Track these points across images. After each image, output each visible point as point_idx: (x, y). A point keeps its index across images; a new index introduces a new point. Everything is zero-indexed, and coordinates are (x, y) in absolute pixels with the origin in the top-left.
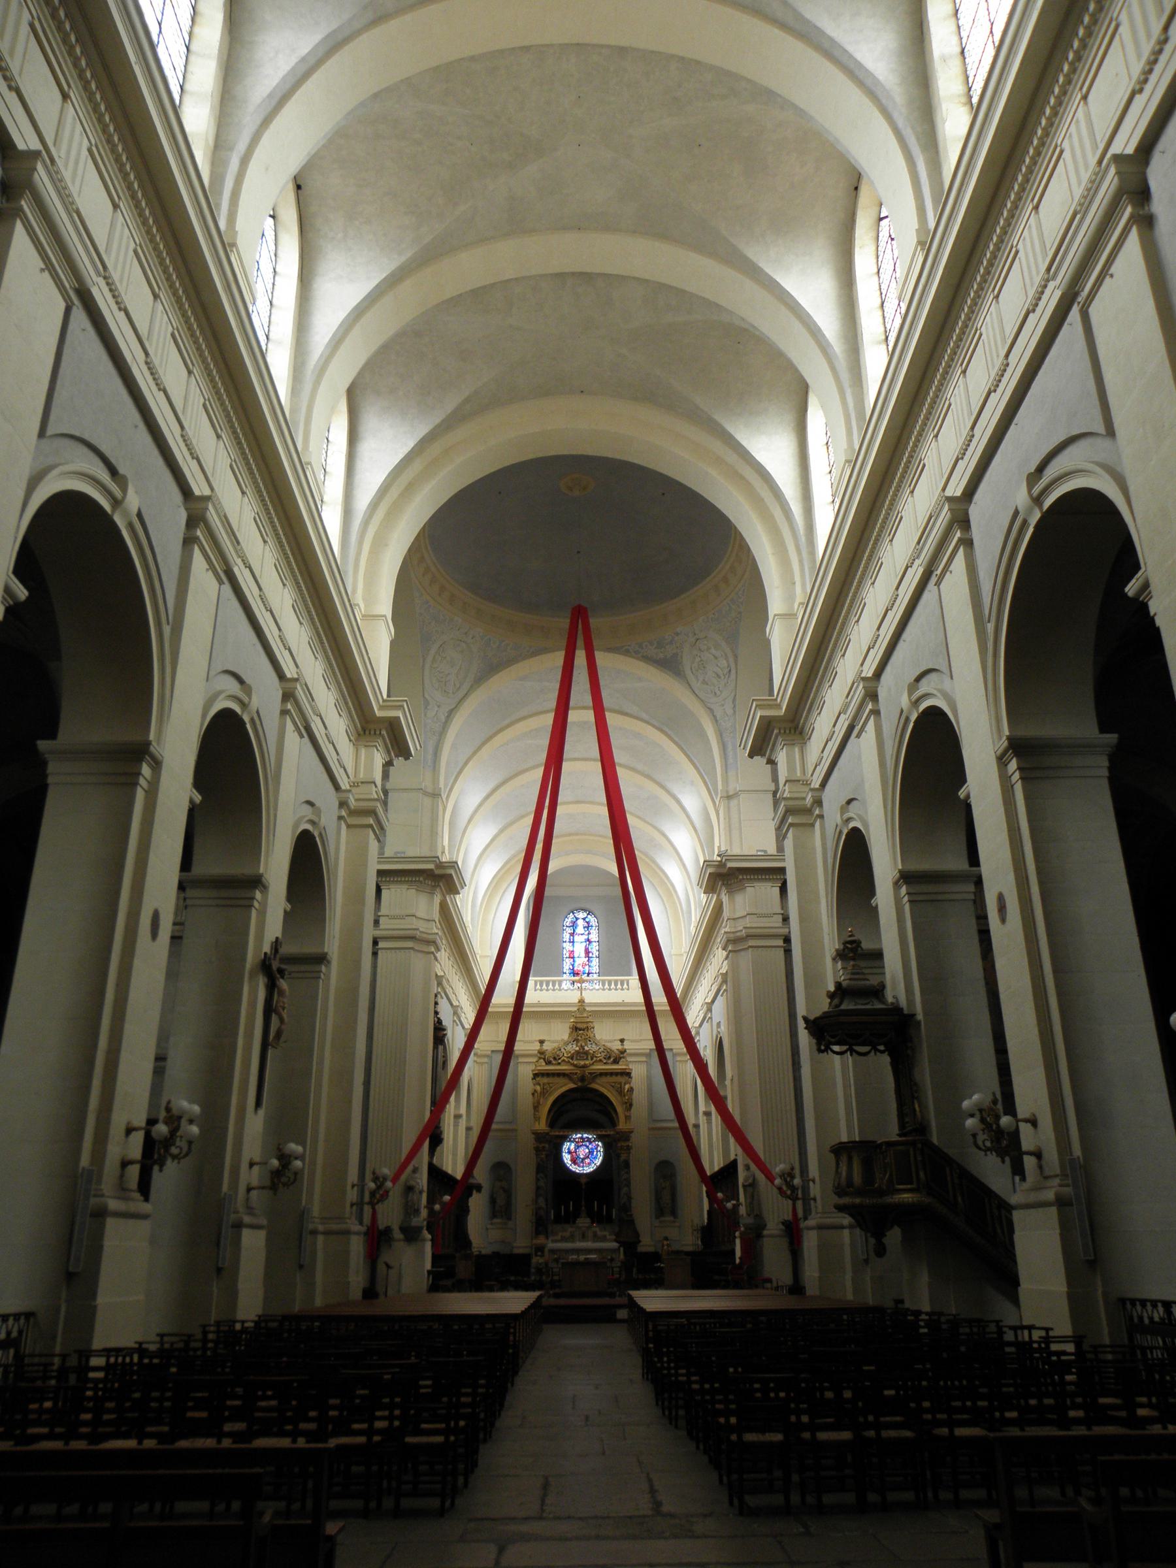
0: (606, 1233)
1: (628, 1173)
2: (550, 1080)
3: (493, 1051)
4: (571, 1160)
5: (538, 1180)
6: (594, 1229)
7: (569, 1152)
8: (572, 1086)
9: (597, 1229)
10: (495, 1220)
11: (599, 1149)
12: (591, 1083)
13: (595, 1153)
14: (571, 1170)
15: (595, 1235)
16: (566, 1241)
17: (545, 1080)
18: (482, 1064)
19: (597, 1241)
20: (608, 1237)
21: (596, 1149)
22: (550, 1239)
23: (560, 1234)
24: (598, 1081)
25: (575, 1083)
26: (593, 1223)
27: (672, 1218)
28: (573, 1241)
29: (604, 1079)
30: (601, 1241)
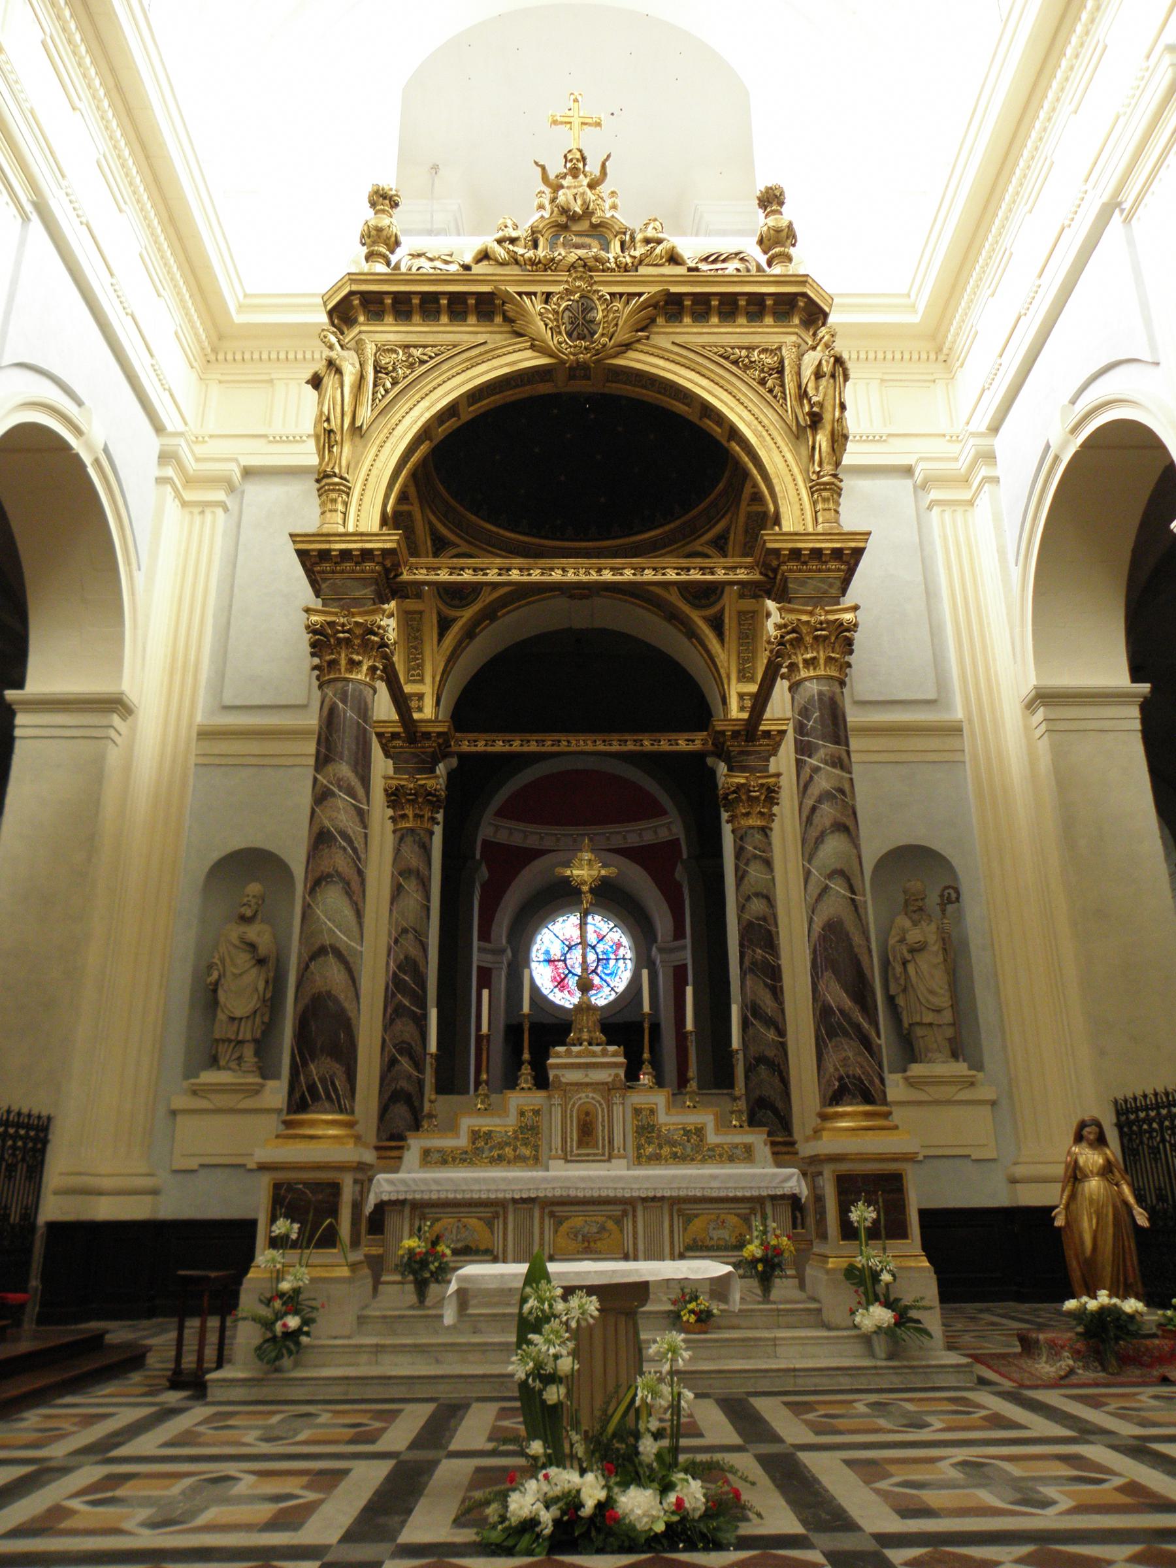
0: (705, 1118)
1: (841, 763)
2: (417, 331)
3: (248, 473)
4: (554, 979)
5: (321, 797)
6: (637, 1099)
7: (550, 961)
8: (529, 360)
9: (659, 1099)
10: (209, 1077)
11: (621, 952)
12: (627, 346)
13: (612, 962)
14: (552, 1004)
15: (646, 1130)
16: (499, 1160)
17: (389, 332)
18: (204, 505)
19: (655, 1159)
20: (712, 1138)
21: (615, 953)
22: (415, 1145)
23: (467, 1123)
24: (666, 336)
25: (536, 346)
26: (632, 1074)
27: (961, 1068)
28: (536, 1161)
29: (691, 332)
30: (680, 1159)
